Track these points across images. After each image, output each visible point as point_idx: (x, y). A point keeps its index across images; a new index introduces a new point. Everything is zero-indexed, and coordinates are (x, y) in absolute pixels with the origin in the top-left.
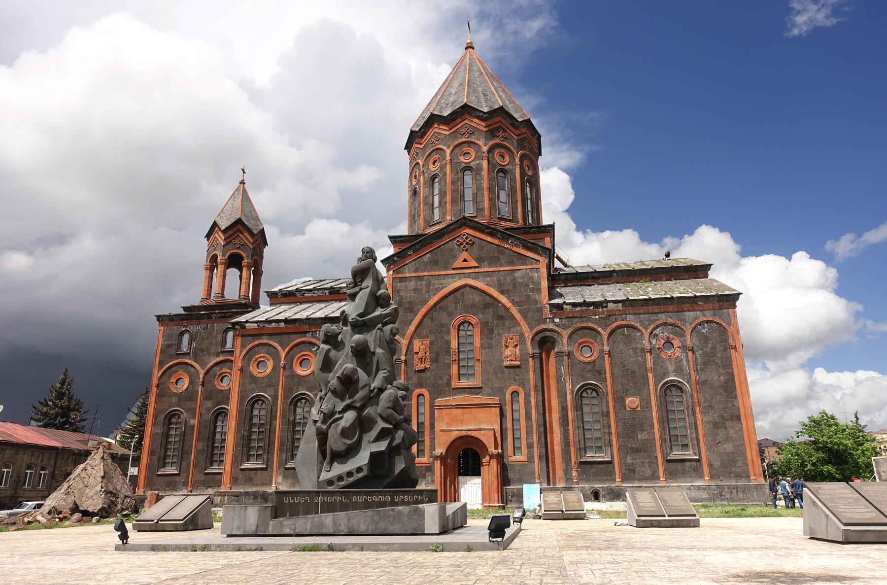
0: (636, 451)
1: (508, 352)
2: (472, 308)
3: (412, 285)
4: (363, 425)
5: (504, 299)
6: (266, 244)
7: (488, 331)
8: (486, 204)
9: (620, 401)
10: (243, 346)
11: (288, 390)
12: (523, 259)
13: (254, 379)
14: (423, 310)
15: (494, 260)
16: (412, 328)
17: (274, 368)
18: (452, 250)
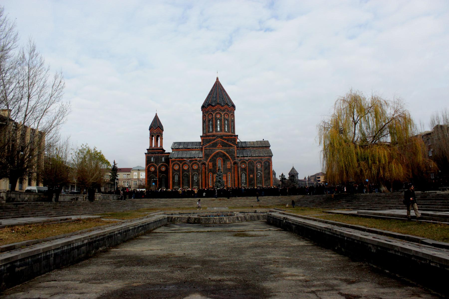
0: (251, 185)
1: (228, 165)
2: (220, 156)
3: (208, 151)
4: (221, 185)
5: (227, 155)
6: (163, 130)
7: (224, 161)
8: (223, 128)
9: (249, 176)
10: (172, 163)
11: (183, 173)
12: (231, 146)
13: (175, 170)
14: (211, 156)
15: (226, 146)
16: (209, 160)
17: (180, 167)
18: (217, 143)
